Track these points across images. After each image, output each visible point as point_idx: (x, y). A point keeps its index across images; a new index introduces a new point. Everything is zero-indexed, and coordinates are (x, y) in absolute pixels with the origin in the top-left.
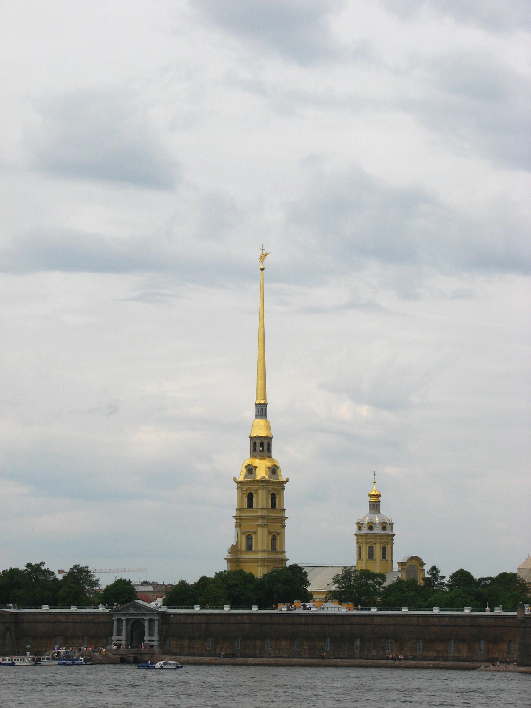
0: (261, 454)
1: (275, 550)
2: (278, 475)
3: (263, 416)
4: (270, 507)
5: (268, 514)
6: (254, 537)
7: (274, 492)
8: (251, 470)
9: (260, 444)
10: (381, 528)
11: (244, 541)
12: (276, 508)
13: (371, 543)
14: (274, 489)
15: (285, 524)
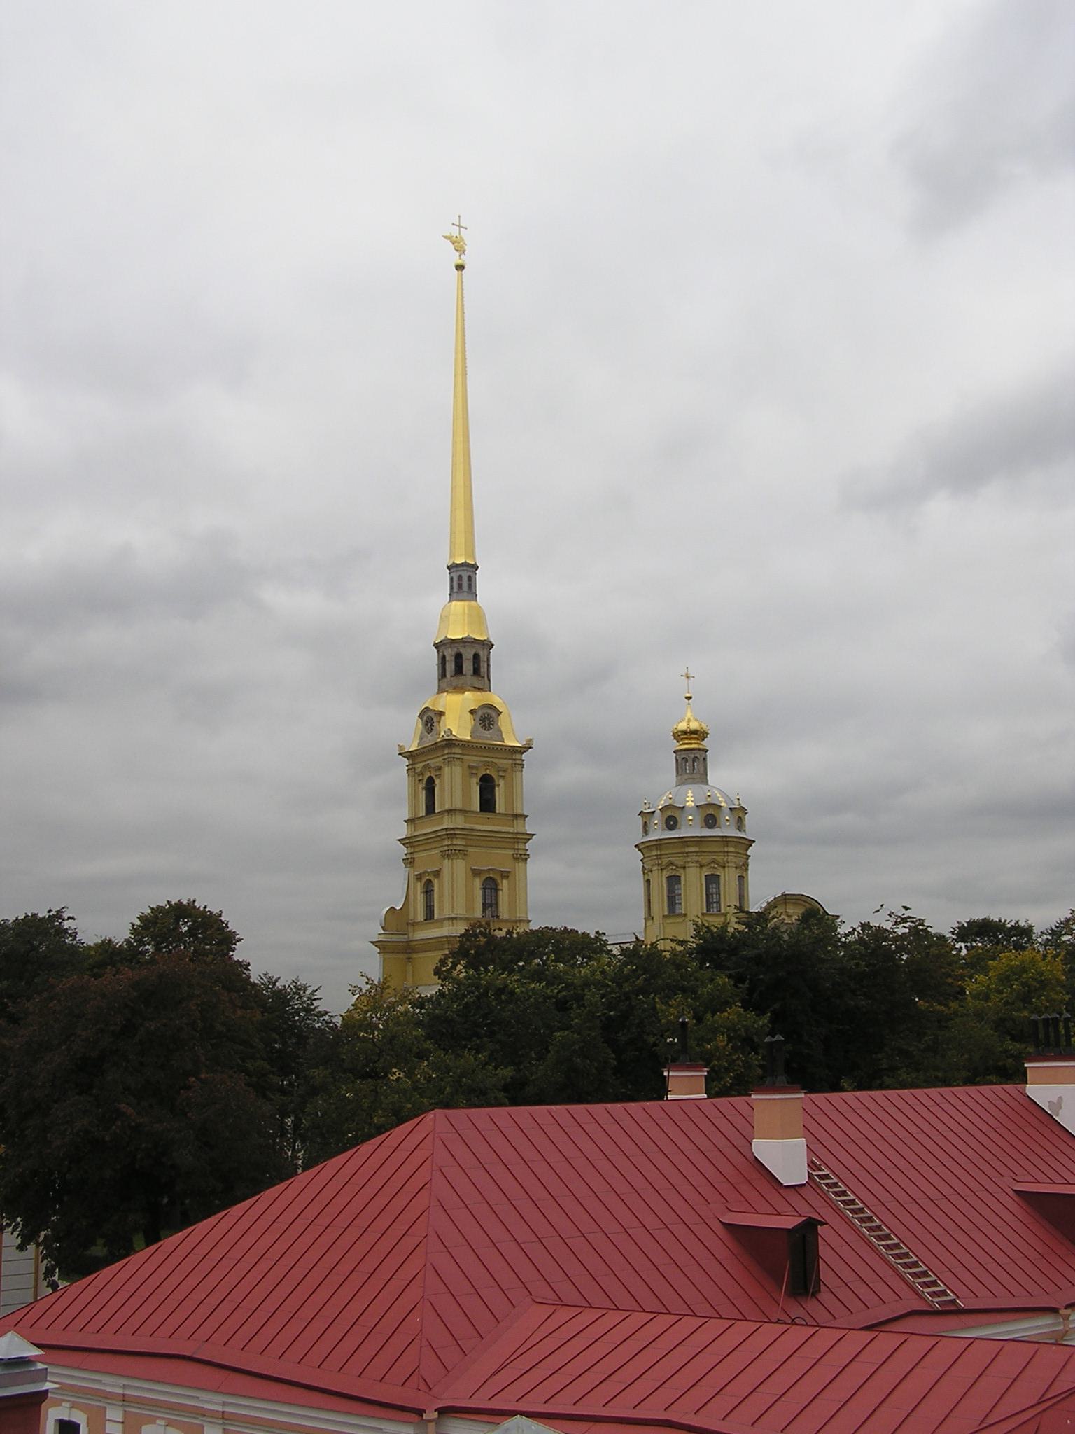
0: (455, 681)
1: (498, 917)
2: (500, 730)
3: (463, 592)
4: (478, 810)
5: (468, 826)
6: (436, 882)
7: (488, 772)
8: (430, 719)
9: (453, 658)
10: (700, 820)
11: (420, 898)
12: (497, 812)
13: (674, 867)
14: (487, 764)
15: (528, 853)
